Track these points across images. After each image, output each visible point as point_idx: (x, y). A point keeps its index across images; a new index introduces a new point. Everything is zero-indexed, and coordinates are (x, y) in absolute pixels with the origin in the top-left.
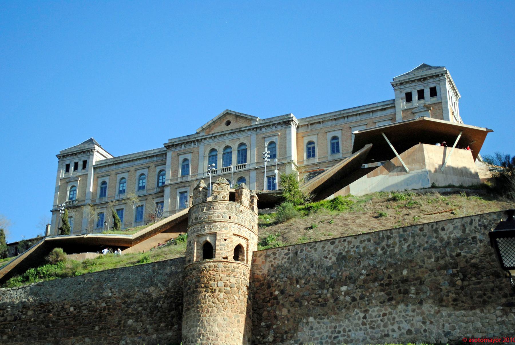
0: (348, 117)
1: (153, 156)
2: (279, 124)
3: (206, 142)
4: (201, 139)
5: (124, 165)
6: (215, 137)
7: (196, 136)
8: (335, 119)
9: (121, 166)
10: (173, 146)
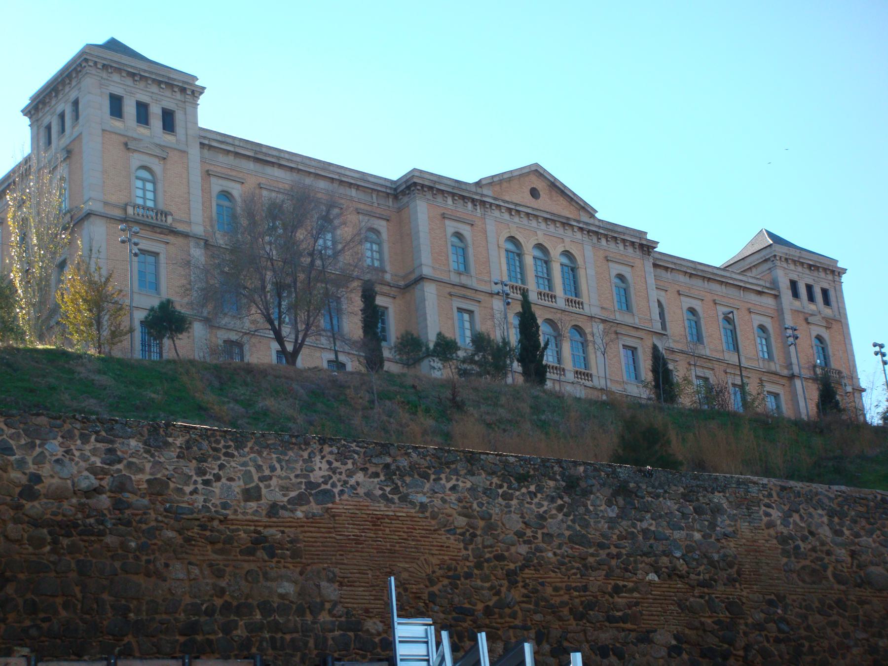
0: (709, 279)
1: (350, 185)
2: (633, 243)
3: (496, 213)
4: (491, 204)
6: (518, 212)
7: (474, 189)
8: (691, 275)
9: (269, 170)
10: (431, 188)
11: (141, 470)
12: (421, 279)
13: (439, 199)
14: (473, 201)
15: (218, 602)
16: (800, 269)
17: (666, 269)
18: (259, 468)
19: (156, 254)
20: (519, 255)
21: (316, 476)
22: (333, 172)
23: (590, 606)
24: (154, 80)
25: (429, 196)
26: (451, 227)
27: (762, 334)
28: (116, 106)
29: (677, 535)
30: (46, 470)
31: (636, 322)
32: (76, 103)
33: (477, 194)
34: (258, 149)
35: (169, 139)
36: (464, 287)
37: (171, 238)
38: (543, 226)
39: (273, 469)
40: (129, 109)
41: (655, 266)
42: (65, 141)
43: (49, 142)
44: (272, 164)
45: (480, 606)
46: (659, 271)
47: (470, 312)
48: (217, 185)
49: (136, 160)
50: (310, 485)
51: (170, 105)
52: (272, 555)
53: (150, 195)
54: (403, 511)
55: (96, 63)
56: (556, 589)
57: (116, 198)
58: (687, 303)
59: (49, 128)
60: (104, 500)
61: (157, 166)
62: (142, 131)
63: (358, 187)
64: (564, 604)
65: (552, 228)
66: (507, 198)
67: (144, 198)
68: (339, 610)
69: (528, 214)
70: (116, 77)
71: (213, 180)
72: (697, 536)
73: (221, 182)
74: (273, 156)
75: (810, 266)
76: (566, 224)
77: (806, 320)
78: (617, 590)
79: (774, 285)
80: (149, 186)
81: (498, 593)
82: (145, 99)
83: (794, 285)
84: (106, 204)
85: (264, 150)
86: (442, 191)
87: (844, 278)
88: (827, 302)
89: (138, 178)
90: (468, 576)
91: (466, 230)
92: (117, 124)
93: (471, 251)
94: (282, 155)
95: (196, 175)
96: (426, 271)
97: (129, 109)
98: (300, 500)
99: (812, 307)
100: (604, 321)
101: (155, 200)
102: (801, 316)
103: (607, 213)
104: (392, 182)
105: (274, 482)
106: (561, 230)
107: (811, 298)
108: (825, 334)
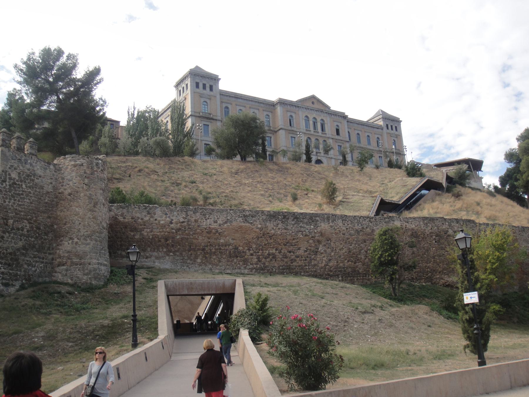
1: (261, 103)
2: (341, 116)
5: (240, 100)
6: (308, 109)
10: (283, 103)
11: (193, 218)
13: (286, 106)
15: (209, 244)
16: (389, 121)
17: (351, 122)
18: (217, 216)
19: (208, 125)
20: (308, 121)
21: (229, 218)
23: (288, 243)
25: (283, 105)
26: (289, 114)
29: (307, 227)
30: (174, 218)
31: (341, 138)
35: (212, 93)
36: (292, 130)
37: (212, 121)
38: (316, 112)
39: (220, 216)
40: (201, 86)
41: (348, 122)
42: (184, 95)
43: (180, 95)
44: (239, 98)
45: (263, 244)
46: (349, 123)
47: (295, 138)
48: (224, 105)
49: (203, 100)
50: (228, 220)
51: (212, 84)
56: (280, 240)
59: (180, 91)
61: (208, 101)
62: (204, 91)
63: (263, 103)
65: (318, 113)
67: (205, 110)
68: (233, 245)
69: (311, 109)
70: (197, 77)
71: (223, 104)
73: (225, 104)
75: (392, 120)
76: (322, 111)
78: (294, 239)
81: (268, 241)
82: (205, 82)
84: (195, 112)
86: (287, 104)
87: (402, 123)
88: (396, 130)
89: (203, 104)
90: (261, 237)
91: (293, 115)
92: (198, 90)
95: (218, 103)
97: (201, 86)
98: (226, 223)
100: (332, 139)
103: (334, 107)
105: (220, 219)
107: (392, 129)
108: (396, 139)
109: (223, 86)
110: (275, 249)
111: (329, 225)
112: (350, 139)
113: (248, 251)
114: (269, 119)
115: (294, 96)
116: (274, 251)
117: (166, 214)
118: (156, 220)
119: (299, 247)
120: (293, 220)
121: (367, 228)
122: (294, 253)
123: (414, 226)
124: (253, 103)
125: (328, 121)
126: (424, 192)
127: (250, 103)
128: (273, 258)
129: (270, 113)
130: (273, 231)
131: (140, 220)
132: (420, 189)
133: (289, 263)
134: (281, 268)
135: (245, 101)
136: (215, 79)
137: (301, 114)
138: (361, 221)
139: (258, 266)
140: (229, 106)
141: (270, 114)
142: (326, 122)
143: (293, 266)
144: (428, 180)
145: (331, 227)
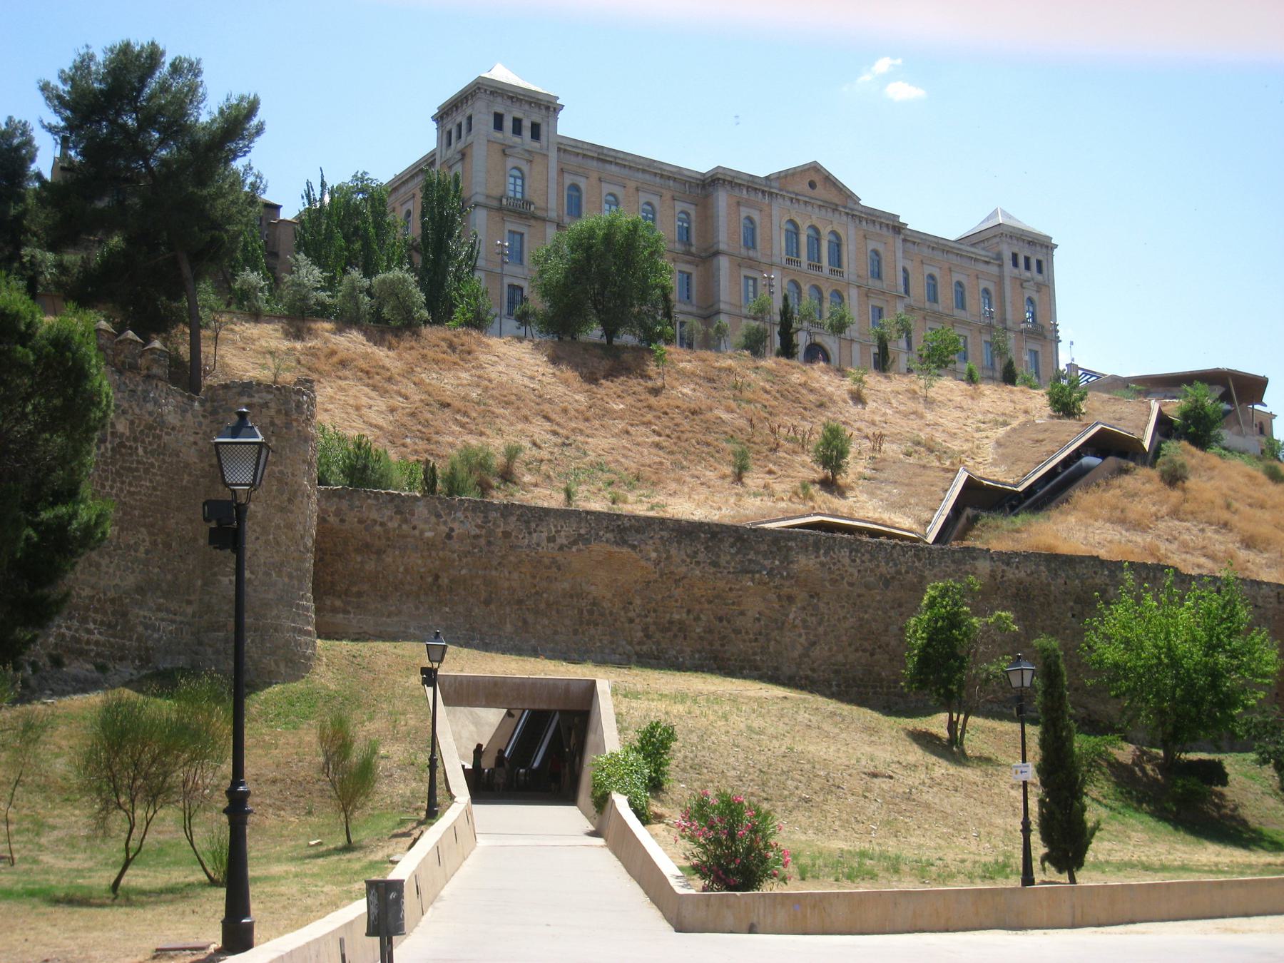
1: (669, 178)
2: (887, 225)
5: (613, 168)
10: (730, 182)
12: (717, 253)
13: (737, 190)
14: (763, 192)
16: (1021, 244)
18: (555, 526)
19: (522, 235)
21: (582, 531)
22: (656, 168)
24: (526, 101)
26: (744, 212)
27: (985, 295)
28: (498, 121)
29: (766, 562)
30: (455, 525)
32: (470, 118)
33: (765, 186)
34: (600, 151)
35: (536, 145)
37: (533, 222)
39: (562, 527)
40: (508, 124)
41: (905, 240)
42: (460, 146)
43: (449, 144)
47: (755, 280)
48: (568, 180)
49: (511, 162)
50: (580, 535)
51: (537, 119)
52: (559, 569)
53: (519, 189)
54: (625, 550)
55: (485, 91)
57: (496, 192)
58: (928, 270)
59: (450, 133)
60: (483, 541)
61: (525, 168)
62: (517, 139)
63: (675, 180)
64: (702, 596)
65: (823, 211)
66: (791, 189)
67: (515, 191)
69: (806, 202)
70: (499, 100)
71: (566, 175)
72: (777, 563)
73: (572, 177)
74: (612, 156)
75: (1029, 243)
76: (835, 209)
77: (1022, 285)
78: (731, 589)
79: (999, 257)
80: (519, 182)
82: (519, 115)
83: (1015, 257)
84: (488, 196)
85: (605, 151)
86: (740, 185)
87: (1056, 251)
88: (1040, 270)
89: (511, 176)
91: (756, 216)
92: (498, 135)
93: (758, 231)
94: (619, 155)
95: (553, 173)
96: (722, 247)
97: (508, 124)
98: (575, 542)
99: (1028, 274)
101: (523, 193)
102: (1018, 283)
103: (869, 199)
104: (704, 174)
105: (563, 533)
106: (830, 214)
107: (1028, 267)
108: (1035, 297)
109: (569, 126)
110: (685, 610)
111: (818, 560)
112: (907, 291)
113: (622, 613)
114: (689, 223)
115: (760, 165)
116: (684, 615)
117: (438, 516)
118: (414, 528)
119: (742, 608)
120: (732, 546)
121: (907, 572)
122: (729, 622)
123: (1023, 574)
124: (647, 177)
125: (851, 236)
126: (1088, 460)
127: (640, 175)
128: (680, 630)
129: (693, 207)
130: (683, 569)
131: (378, 528)
132: (1077, 454)
133: (717, 645)
134: (697, 656)
135: (626, 172)
136: (550, 107)
137: (778, 216)
138: (895, 555)
139: (645, 648)
140: (582, 183)
141: (692, 210)
142: (844, 238)
143: (725, 652)
144: (1102, 430)
145: (823, 564)
